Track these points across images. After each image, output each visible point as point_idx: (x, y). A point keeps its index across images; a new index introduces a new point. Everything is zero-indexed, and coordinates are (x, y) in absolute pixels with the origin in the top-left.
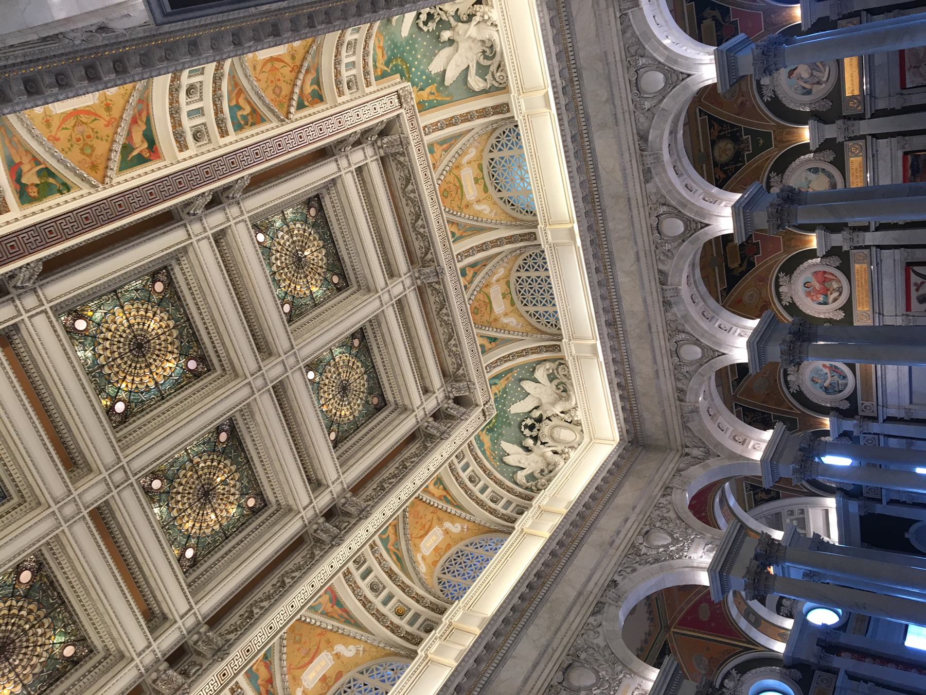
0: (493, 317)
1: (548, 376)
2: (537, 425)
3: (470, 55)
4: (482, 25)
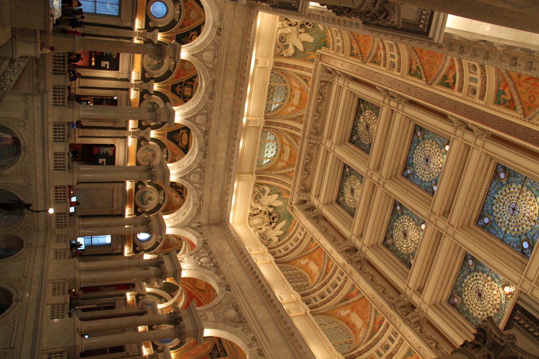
0: (302, 91)
1: (288, 48)
2: (304, 23)
3: (265, 199)
4: (256, 208)
